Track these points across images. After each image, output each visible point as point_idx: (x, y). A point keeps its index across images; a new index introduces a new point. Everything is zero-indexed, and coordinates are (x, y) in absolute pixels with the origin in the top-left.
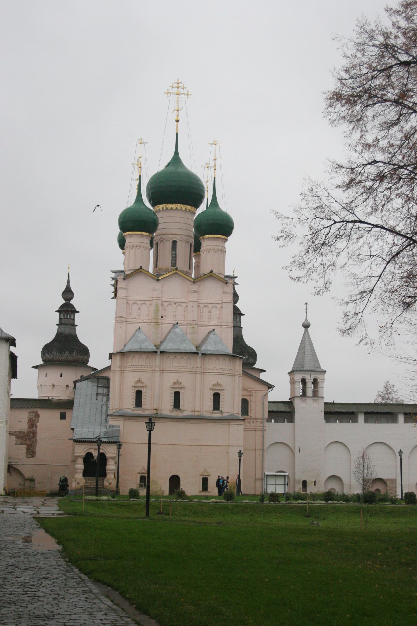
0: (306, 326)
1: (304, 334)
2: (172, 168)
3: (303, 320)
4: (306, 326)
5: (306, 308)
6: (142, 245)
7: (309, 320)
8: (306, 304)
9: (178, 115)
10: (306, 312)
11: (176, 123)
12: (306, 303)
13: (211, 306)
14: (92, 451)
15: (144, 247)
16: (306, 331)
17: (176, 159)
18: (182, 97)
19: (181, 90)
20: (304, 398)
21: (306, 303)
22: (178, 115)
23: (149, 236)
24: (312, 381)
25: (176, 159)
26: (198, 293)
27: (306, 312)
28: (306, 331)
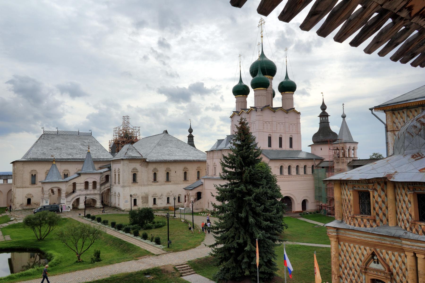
0: (344, 117)
1: (343, 122)
2: (261, 59)
3: (342, 114)
4: (344, 117)
6: (238, 101)
7: (345, 113)
9: (262, 34)
10: (343, 109)
11: (261, 38)
12: (343, 104)
13: (253, 123)
14: (188, 193)
15: (239, 102)
17: (263, 55)
18: (263, 25)
19: (262, 22)
21: (343, 104)
22: (262, 34)
23: (243, 96)
25: (263, 55)
26: (250, 118)
27: (343, 109)
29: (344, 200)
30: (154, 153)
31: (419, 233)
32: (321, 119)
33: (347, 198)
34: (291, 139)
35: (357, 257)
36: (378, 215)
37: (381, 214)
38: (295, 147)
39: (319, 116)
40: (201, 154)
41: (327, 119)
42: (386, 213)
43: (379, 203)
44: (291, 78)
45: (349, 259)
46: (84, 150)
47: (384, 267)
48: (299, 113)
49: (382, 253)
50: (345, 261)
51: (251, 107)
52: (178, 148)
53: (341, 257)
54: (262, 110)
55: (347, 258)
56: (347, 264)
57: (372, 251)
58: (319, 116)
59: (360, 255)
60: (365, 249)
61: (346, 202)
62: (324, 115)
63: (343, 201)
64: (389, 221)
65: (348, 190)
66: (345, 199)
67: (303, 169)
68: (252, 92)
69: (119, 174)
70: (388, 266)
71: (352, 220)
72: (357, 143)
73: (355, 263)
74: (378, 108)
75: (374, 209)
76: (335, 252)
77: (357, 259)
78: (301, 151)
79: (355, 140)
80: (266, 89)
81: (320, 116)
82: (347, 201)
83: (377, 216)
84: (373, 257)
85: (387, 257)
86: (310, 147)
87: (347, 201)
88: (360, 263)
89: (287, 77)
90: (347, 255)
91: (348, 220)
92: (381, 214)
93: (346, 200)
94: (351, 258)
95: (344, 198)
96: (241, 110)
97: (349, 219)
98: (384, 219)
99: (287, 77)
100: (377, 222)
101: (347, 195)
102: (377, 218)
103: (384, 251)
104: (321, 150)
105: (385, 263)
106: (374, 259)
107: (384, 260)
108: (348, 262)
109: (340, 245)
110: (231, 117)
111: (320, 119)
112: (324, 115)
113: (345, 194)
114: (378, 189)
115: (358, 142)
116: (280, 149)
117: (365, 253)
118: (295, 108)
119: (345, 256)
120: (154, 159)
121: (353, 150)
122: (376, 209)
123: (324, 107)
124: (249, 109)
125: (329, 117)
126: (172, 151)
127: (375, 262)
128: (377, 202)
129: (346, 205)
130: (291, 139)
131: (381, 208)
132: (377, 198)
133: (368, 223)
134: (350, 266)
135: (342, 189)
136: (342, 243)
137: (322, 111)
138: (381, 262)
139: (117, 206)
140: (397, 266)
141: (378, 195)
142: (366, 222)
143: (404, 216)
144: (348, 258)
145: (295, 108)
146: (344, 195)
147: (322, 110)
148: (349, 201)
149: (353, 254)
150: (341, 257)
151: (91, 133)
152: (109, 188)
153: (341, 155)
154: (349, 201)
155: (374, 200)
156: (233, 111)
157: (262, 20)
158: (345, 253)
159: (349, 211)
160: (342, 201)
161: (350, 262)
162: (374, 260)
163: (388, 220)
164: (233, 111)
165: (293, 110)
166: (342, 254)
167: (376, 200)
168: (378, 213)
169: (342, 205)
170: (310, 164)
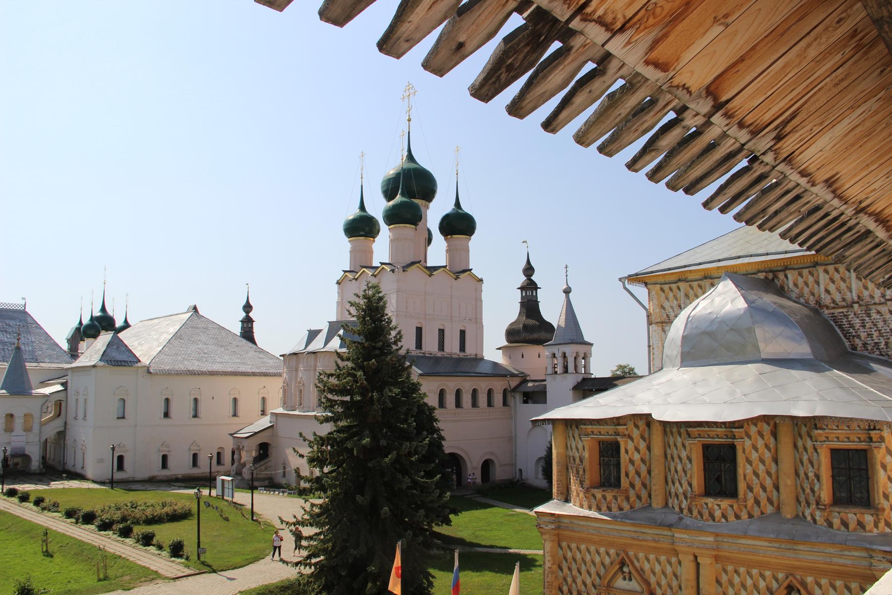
0: (567, 291)
4: (567, 291)
5: (567, 271)
8: (566, 267)
9: (409, 116)
10: (567, 276)
12: (566, 265)
14: (239, 444)
16: (568, 298)
17: (410, 157)
18: (411, 96)
20: (566, 375)
21: (566, 265)
22: (409, 116)
24: (560, 355)
27: (567, 276)
28: (568, 298)
29: (572, 459)
30: (166, 355)
31: (704, 518)
32: (524, 294)
33: (577, 455)
34: (463, 333)
35: (593, 570)
36: (632, 485)
37: (638, 482)
38: (470, 350)
39: (519, 288)
40: (270, 361)
41: (534, 294)
42: (648, 483)
43: (636, 464)
44: (466, 208)
45: (578, 574)
46: (5, 342)
47: (640, 585)
48: (481, 280)
49: (638, 560)
50: (569, 580)
51: (382, 264)
52: (221, 346)
53: (562, 572)
54: (404, 271)
55: (573, 574)
56: (574, 585)
57: (620, 557)
58: (519, 288)
59: (597, 566)
60: (608, 554)
61: (575, 463)
62: (530, 287)
63: (570, 460)
64: (653, 497)
65: (580, 438)
66: (573, 456)
67: (485, 396)
68: (384, 229)
69: (86, 399)
70: (647, 583)
71: (585, 499)
72: (592, 344)
73: (588, 581)
74: (635, 278)
75: (627, 475)
76: (551, 562)
77: (592, 573)
78: (482, 359)
79: (587, 338)
80: (414, 226)
81: (522, 288)
82: (577, 460)
83: (631, 489)
84: (621, 568)
85: (647, 566)
86: (501, 351)
87: (577, 460)
88: (598, 581)
89: (458, 204)
90: (574, 567)
91: (578, 498)
92: (638, 482)
93: (574, 460)
94: (580, 573)
95: (571, 454)
96: (360, 268)
97: (579, 497)
98: (644, 494)
99: (458, 204)
100: (632, 500)
101: (577, 449)
102: (632, 493)
103: (641, 555)
104: (523, 357)
105: (643, 578)
106: (623, 572)
107: (641, 572)
108: (574, 581)
109: (562, 549)
110: (338, 283)
111: (522, 294)
112: (530, 287)
113: (574, 446)
114: (634, 436)
115: (591, 342)
116: (462, 354)
117: (607, 561)
118: (472, 269)
119: (570, 569)
120: (167, 368)
121: (583, 358)
122: (631, 475)
123: (529, 270)
124: (377, 268)
125: (538, 290)
126: (206, 351)
127: (624, 579)
128: (632, 462)
129: (574, 469)
130: (463, 333)
131: (638, 473)
132: (633, 453)
133: (615, 503)
134: (579, 589)
135: (569, 436)
136: (564, 544)
137: (526, 278)
138: (635, 577)
139: (79, 471)
140: (664, 582)
141: (634, 448)
142: (611, 500)
143: (679, 487)
144: (575, 572)
145: (472, 269)
146: (572, 449)
147: (526, 276)
148: (581, 460)
149: (585, 564)
150: (562, 572)
151: (25, 305)
152: (62, 429)
153: (559, 369)
154: (581, 460)
155: (627, 457)
156: (343, 271)
157: (411, 86)
158: (571, 563)
159: (580, 480)
160: (568, 460)
161: (579, 581)
162: (623, 574)
163: (650, 496)
164: (343, 271)
165: (469, 272)
166: (565, 565)
167: (630, 458)
168: (632, 482)
169: (568, 469)
170: (499, 386)
